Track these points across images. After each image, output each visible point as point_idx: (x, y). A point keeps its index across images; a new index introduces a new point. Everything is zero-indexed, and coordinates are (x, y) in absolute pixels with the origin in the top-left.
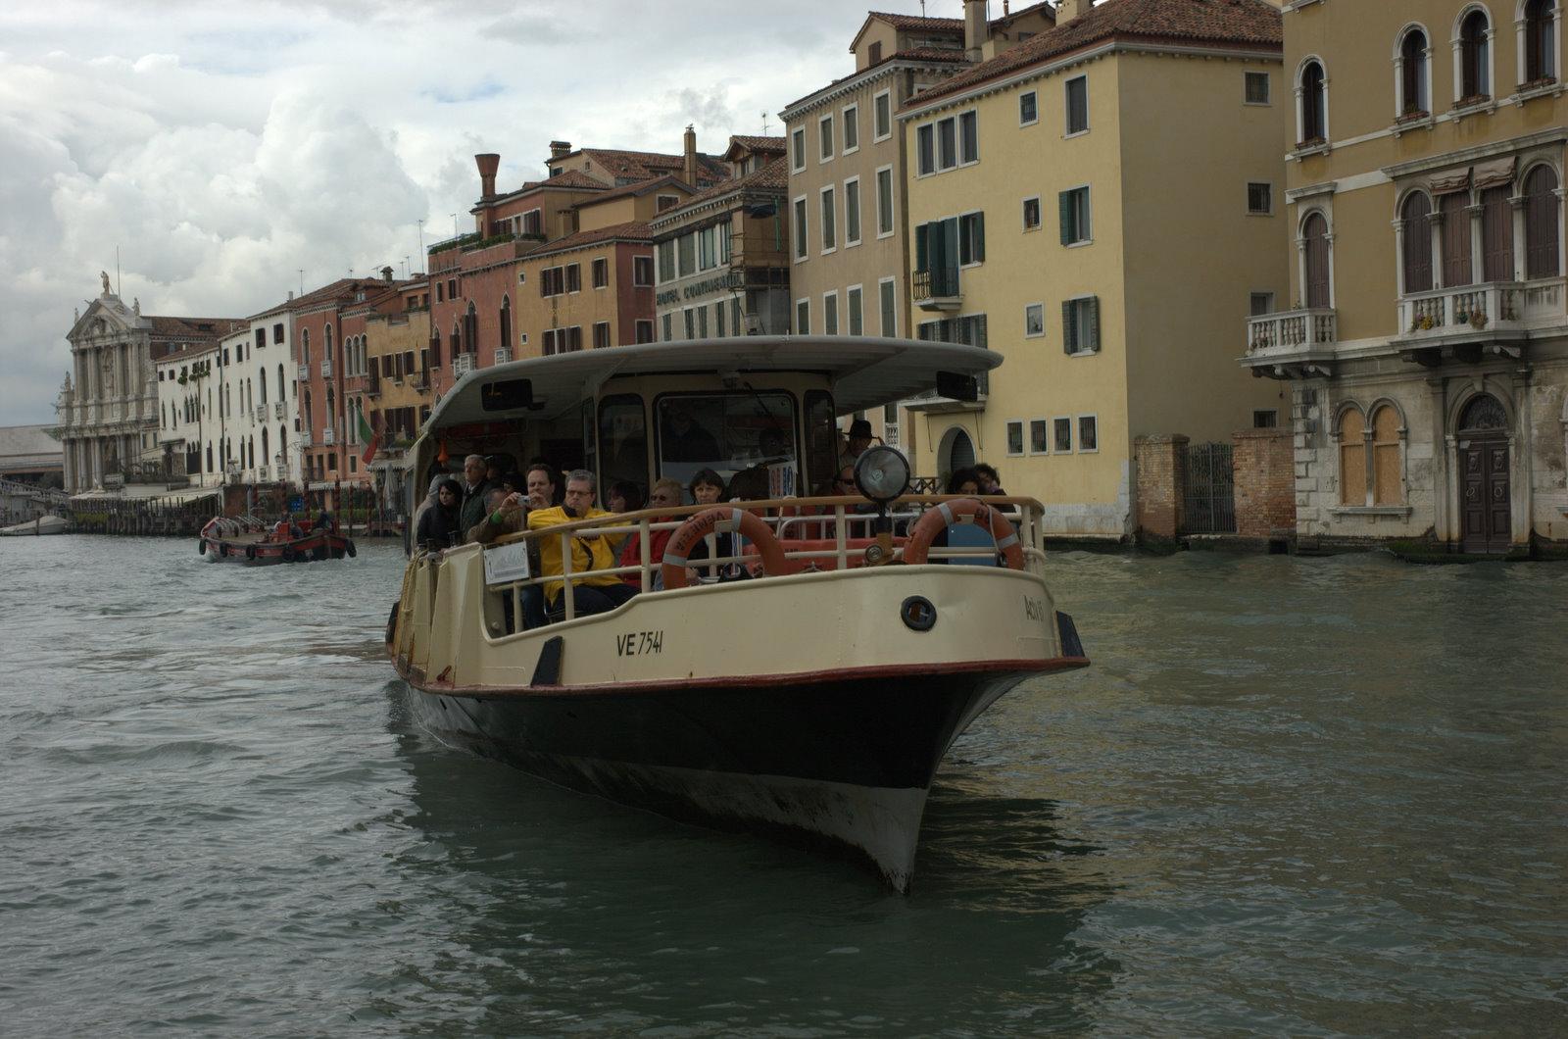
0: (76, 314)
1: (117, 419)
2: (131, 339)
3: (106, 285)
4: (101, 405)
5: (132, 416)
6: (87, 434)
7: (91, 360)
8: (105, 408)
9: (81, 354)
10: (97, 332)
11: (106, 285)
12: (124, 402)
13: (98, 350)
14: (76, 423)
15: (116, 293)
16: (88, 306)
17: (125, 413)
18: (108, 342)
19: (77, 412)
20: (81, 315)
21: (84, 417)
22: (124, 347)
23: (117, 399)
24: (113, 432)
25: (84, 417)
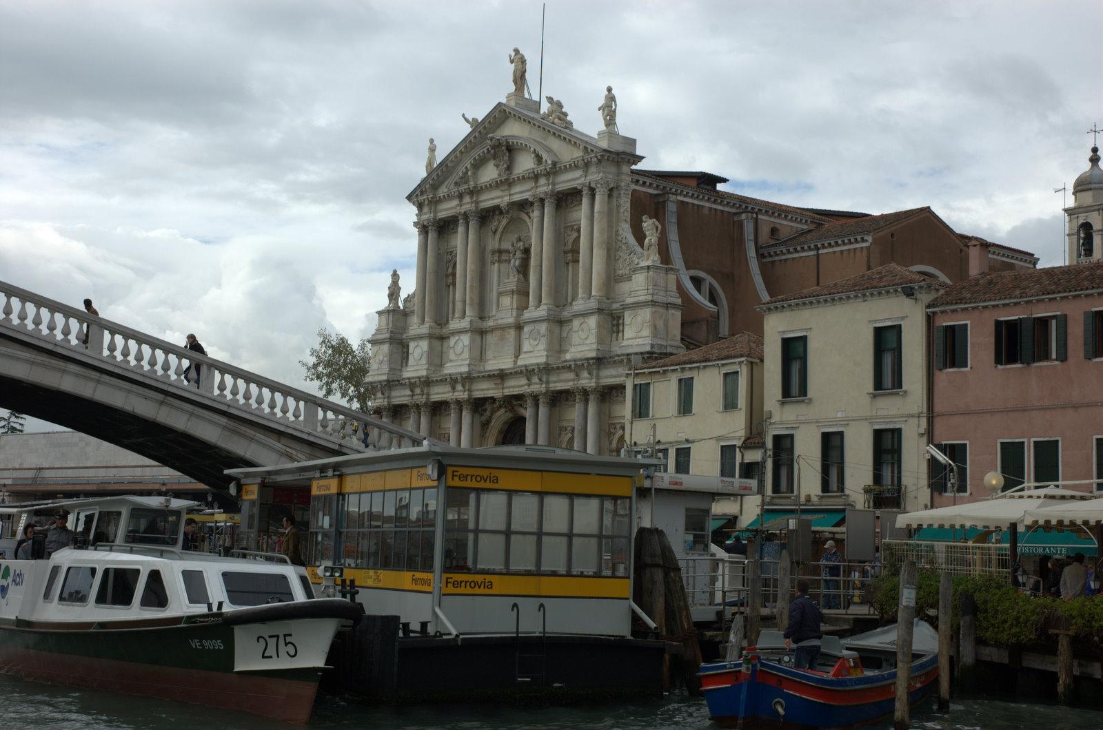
0: (432, 150)
1: (535, 352)
2: (594, 176)
3: (520, 79)
4: (482, 333)
5: (584, 340)
6: (439, 393)
7: (463, 243)
8: (491, 339)
9: (436, 230)
10: (490, 173)
11: (520, 79)
12: (558, 321)
13: (485, 216)
14: (417, 367)
15: (536, 98)
16: (467, 129)
17: (558, 344)
18: (520, 193)
19: (419, 351)
20: (439, 157)
21: (437, 358)
22: (566, 200)
23: (542, 311)
24: (516, 386)
25: (437, 358)
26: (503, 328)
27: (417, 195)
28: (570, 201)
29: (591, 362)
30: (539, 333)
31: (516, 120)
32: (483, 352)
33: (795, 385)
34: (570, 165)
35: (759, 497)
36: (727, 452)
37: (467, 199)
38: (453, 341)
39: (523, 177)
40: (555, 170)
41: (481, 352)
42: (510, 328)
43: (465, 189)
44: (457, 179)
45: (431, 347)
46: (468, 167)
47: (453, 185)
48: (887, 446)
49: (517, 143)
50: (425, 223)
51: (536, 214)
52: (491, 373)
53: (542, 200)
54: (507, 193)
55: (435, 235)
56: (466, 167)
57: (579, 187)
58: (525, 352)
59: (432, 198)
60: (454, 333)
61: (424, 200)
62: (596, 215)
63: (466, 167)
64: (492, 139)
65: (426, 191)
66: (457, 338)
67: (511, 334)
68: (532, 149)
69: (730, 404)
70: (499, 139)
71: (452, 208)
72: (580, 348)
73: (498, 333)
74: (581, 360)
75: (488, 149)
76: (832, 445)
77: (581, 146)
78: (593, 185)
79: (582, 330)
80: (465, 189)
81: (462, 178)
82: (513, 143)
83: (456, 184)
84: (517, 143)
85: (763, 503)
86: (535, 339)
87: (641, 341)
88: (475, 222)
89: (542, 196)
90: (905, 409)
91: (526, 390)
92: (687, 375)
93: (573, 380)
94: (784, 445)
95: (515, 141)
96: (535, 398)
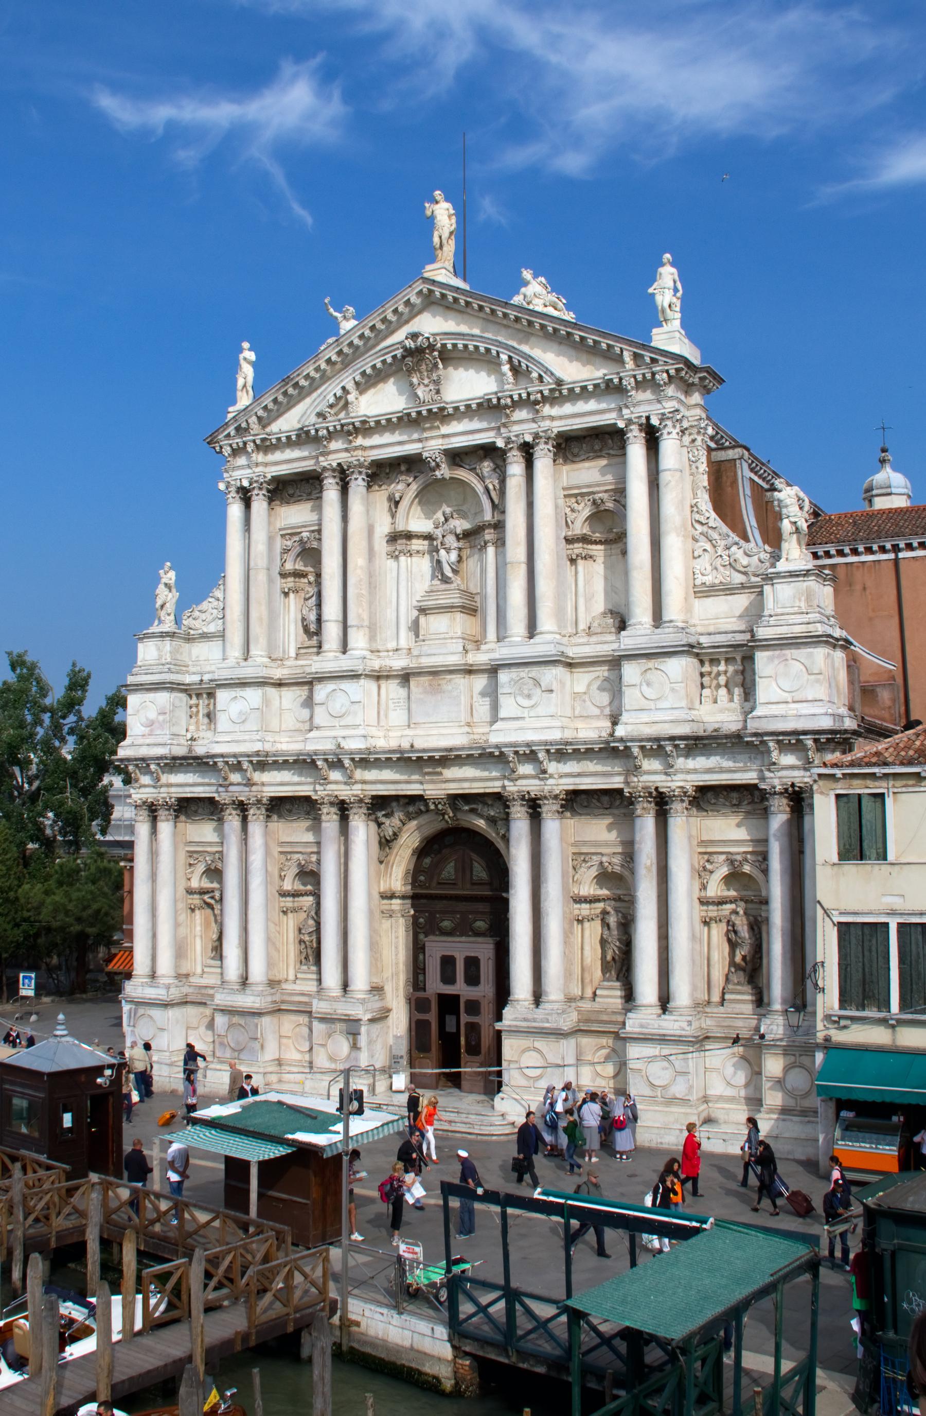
13: (381, 471)
26: (435, 673)
27: (228, 435)
28: (576, 451)
29: (682, 744)
30: (537, 683)
31: (448, 308)
32: (382, 713)
34: (596, 386)
38: (321, 692)
39: (479, 405)
40: (560, 394)
41: (379, 713)
42: (451, 672)
43: (342, 426)
44: (323, 407)
45: (266, 701)
46: (350, 386)
47: (313, 419)
49: (466, 346)
50: (246, 483)
51: (516, 468)
52: (425, 756)
53: (527, 450)
54: (434, 433)
55: (265, 504)
56: (344, 388)
57: (621, 424)
58: (502, 719)
59: (263, 440)
60: (321, 679)
61: (245, 443)
62: (665, 478)
63: (344, 388)
64: (414, 336)
65: (247, 430)
66: (330, 686)
68: (504, 357)
70: (428, 338)
72: (645, 717)
73: (424, 679)
74: (649, 740)
75: (394, 357)
78: (655, 421)
79: (648, 684)
80: (342, 426)
81: (331, 406)
82: (455, 345)
83: (320, 415)
84: (466, 346)
86: (529, 696)
87: (805, 709)
88: (360, 482)
89: (529, 438)
91: (512, 788)
96: (534, 806)
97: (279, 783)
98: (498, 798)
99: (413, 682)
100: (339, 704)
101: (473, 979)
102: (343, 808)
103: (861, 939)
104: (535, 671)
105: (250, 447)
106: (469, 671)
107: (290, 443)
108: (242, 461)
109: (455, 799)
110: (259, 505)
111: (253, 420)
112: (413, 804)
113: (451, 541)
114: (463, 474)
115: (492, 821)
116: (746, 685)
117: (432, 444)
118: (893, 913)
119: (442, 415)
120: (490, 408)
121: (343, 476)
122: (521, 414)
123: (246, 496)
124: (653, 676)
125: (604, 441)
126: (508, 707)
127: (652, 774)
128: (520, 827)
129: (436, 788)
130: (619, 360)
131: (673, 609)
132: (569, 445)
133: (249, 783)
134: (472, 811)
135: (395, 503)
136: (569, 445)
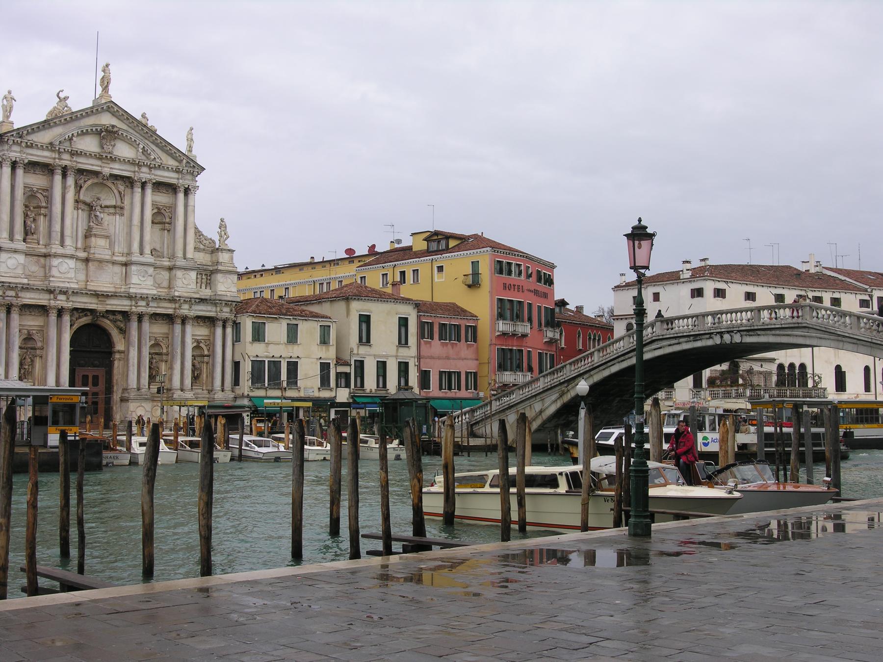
13: (80, 172)
18: (117, 169)
26: (100, 261)
30: (146, 272)
33: (365, 339)
35: (347, 390)
36: (325, 367)
37: (66, 156)
38: (55, 262)
48: (403, 368)
53: (143, 185)
60: (56, 256)
66: (60, 260)
67: (110, 265)
69: (324, 341)
71: (46, 157)
76: (382, 367)
77: (184, 161)
85: (350, 393)
90: (409, 354)
91: (134, 309)
92: (295, 322)
93: (175, 309)
94: (360, 366)
95: (125, 134)
96: (140, 317)
97: (29, 298)
98: (126, 315)
99: (90, 264)
100: (64, 268)
101: (95, 384)
102: (60, 312)
103: (258, 365)
104: (146, 268)
105: (24, 145)
106: (114, 263)
107: (42, 148)
108: (16, 148)
109: (107, 311)
110: (20, 172)
111: (25, 132)
112: (84, 311)
113: (98, 208)
114: (109, 184)
115: (114, 321)
116: (209, 284)
117: (106, 171)
118: (267, 357)
119: (113, 160)
120: (132, 163)
121: (65, 171)
122: (144, 169)
123: (14, 165)
124: (186, 276)
125: (172, 188)
126: (135, 279)
127: (185, 310)
128: (134, 325)
129: (100, 308)
130: (180, 162)
131: (190, 255)
132: (159, 186)
133: (17, 297)
134: (107, 318)
135: (78, 188)
136: (159, 186)
